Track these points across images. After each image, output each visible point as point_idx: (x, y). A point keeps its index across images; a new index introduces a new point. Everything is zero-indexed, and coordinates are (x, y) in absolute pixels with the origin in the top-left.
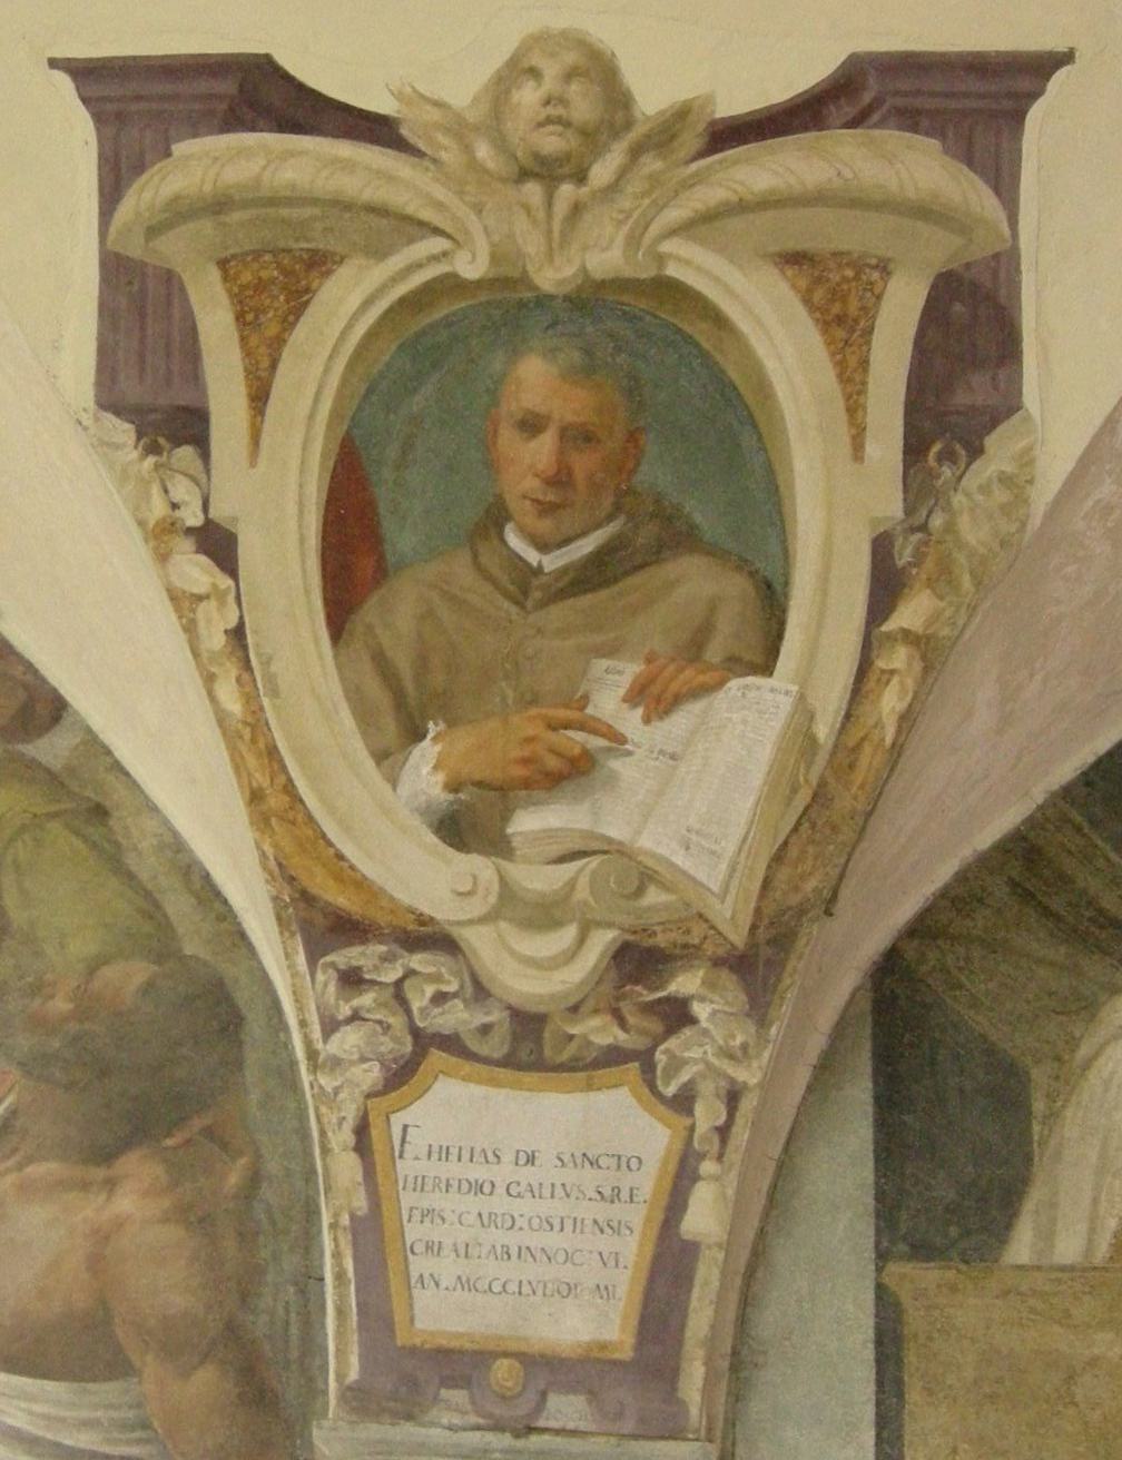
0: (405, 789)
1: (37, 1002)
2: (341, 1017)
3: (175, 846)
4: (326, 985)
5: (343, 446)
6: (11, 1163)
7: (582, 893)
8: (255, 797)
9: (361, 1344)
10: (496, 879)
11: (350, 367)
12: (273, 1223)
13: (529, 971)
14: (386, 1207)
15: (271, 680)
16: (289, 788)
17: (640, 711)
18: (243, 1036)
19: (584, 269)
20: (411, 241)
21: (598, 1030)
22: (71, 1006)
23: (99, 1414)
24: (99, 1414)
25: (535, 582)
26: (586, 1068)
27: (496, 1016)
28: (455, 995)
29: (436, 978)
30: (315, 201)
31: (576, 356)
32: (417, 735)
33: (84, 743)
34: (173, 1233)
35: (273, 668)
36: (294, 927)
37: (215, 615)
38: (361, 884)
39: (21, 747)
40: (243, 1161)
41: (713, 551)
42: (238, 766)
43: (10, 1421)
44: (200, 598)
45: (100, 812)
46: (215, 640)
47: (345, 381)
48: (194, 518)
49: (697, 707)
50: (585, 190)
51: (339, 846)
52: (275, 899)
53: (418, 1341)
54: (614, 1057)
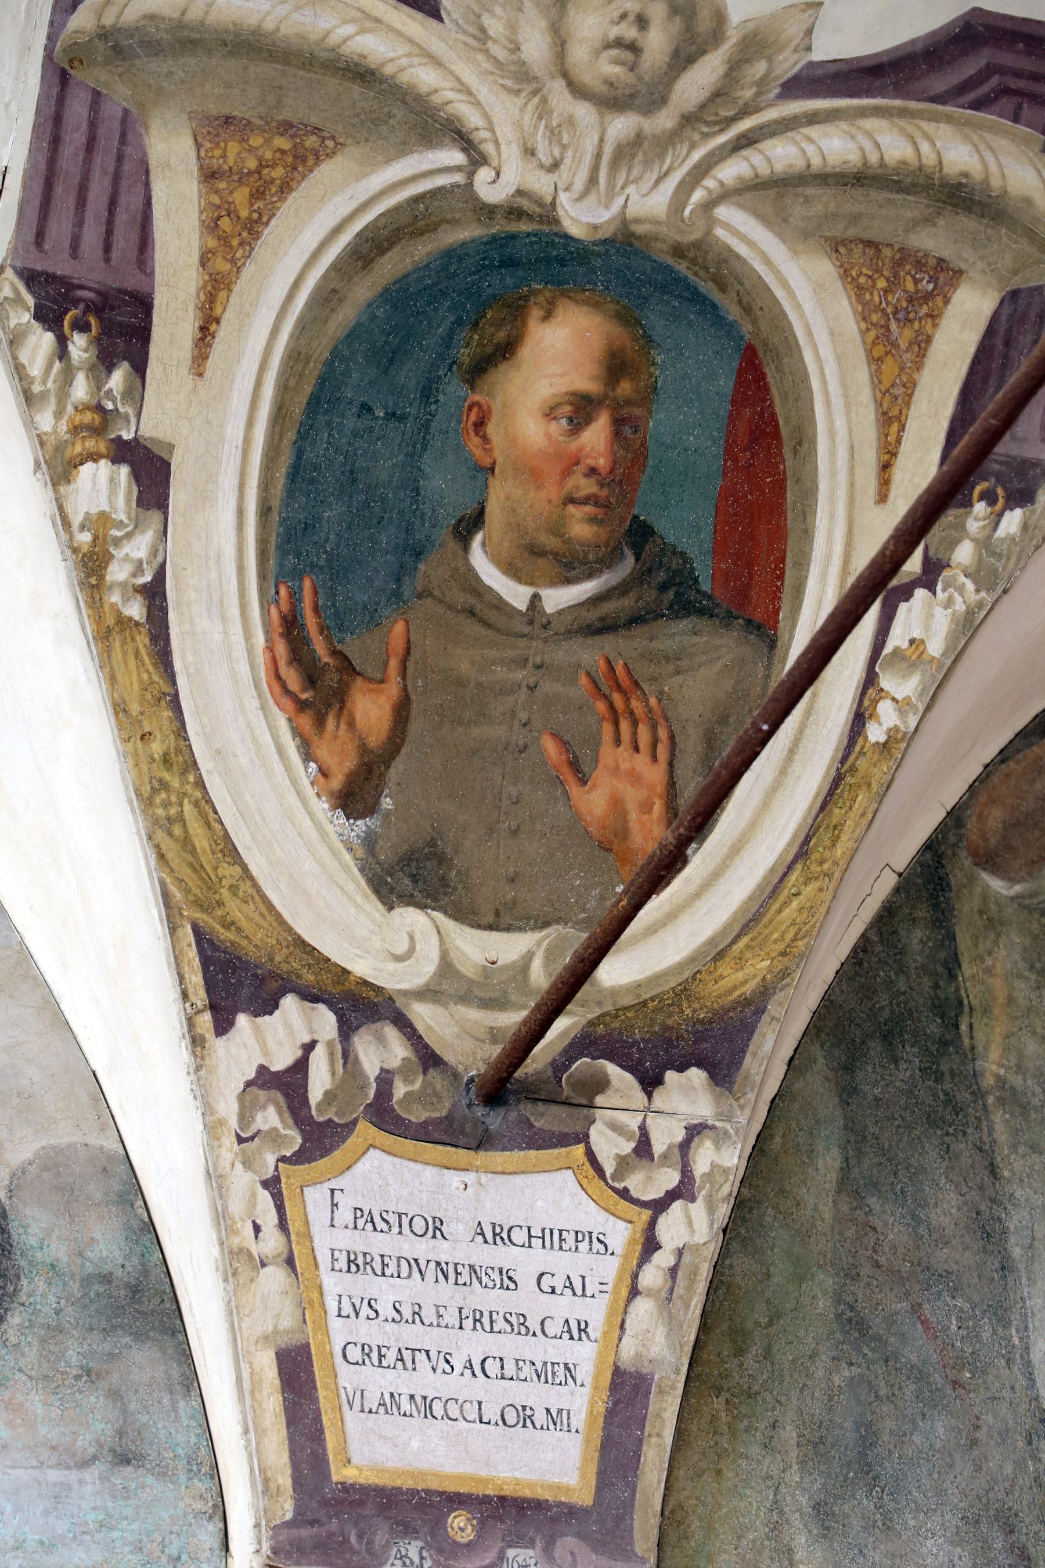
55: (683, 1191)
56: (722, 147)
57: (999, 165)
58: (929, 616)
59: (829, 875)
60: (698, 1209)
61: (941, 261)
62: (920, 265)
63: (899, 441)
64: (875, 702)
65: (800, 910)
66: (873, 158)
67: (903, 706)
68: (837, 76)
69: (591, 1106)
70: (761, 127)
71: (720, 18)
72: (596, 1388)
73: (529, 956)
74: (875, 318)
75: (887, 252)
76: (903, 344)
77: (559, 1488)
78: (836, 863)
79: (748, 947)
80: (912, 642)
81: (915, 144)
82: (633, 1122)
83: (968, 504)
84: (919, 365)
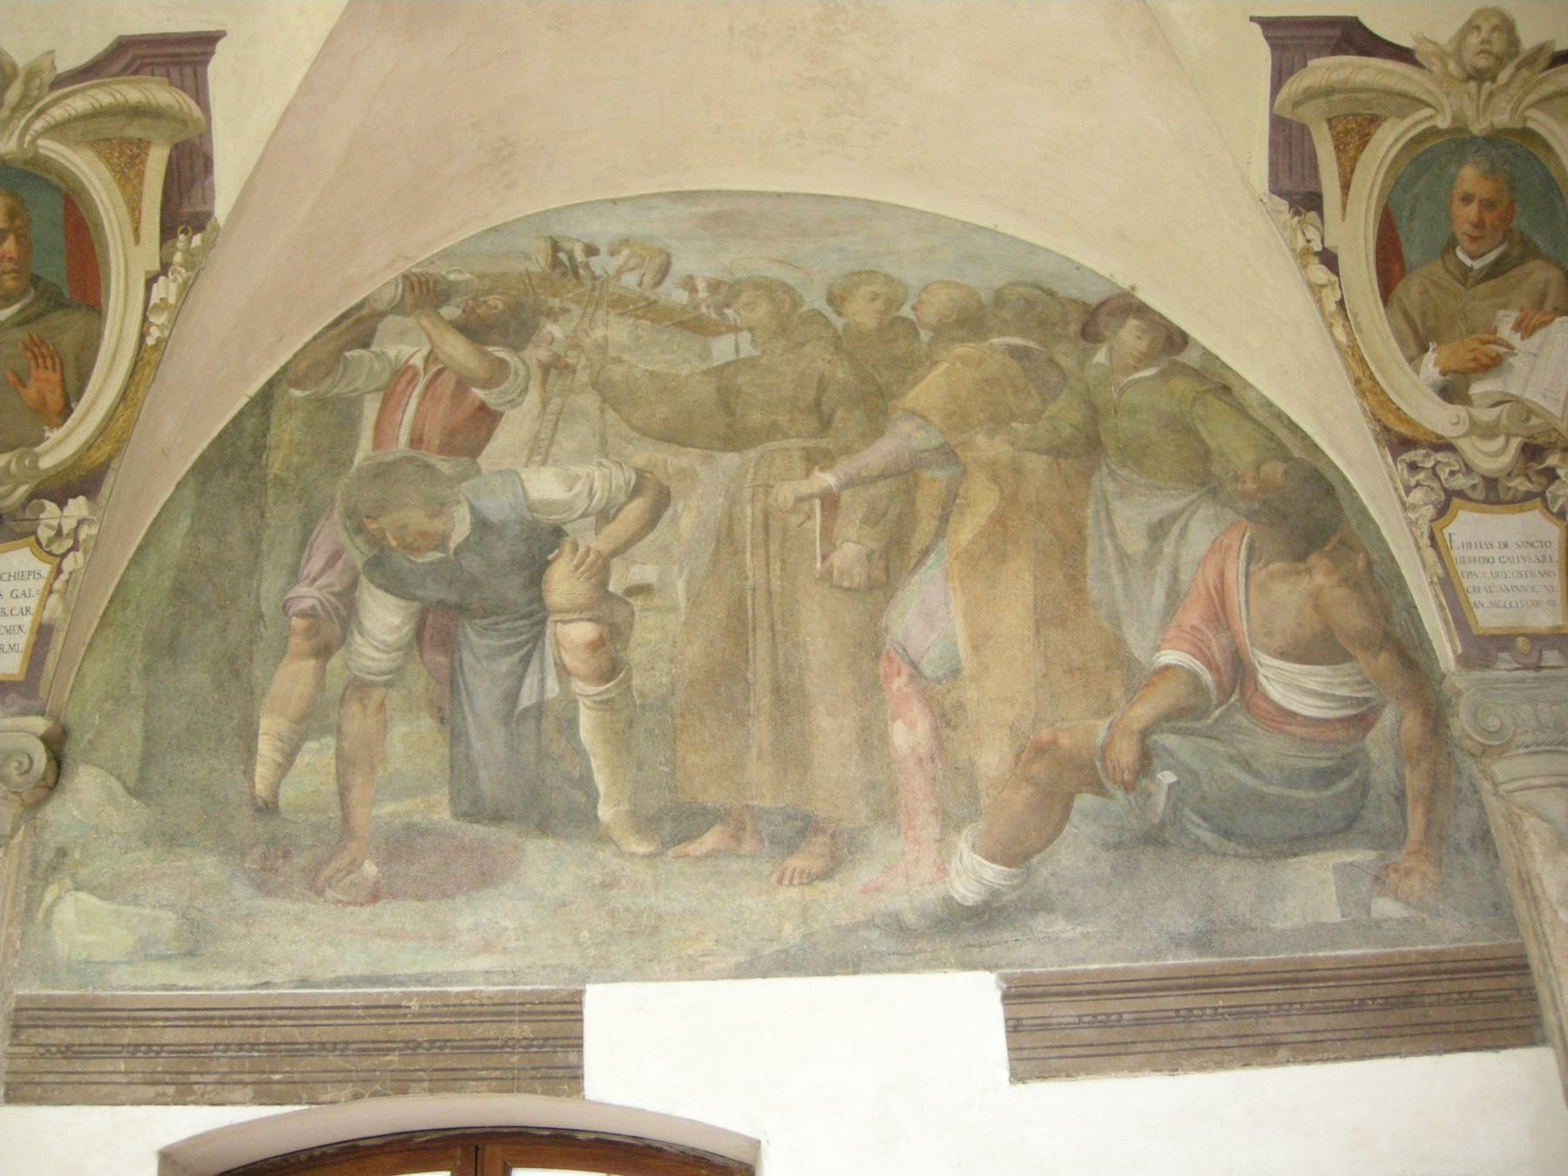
0: (1423, 375)
1: (1239, 486)
6: (1261, 564)
7: (1504, 421)
8: (1357, 382)
9: (1459, 635)
10: (1467, 416)
11: (1387, 172)
13: (1489, 459)
14: (1451, 571)
15: (1358, 324)
16: (1372, 377)
17: (1519, 335)
19: (1492, 123)
20: (1417, 110)
21: (1521, 484)
22: (1255, 486)
23: (1347, 679)
24: (1347, 679)
25: (1470, 274)
26: (1519, 502)
27: (1477, 480)
28: (1458, 471)
29: (1449, 464)
30: (1374, 90)
31: (1487, 166)
32: (1425, 349)
35: (1359, 319)
37: (1331, 295)
38: (1409, 422)
39: (1178, 358)
40: (1361, 555)
41: (1547, 259)
42: (1348, 368)
43: (1309, 686)
44: (1322, 286)
45: (1226, 389)
46: (1331, 306)
47: (1385, 178)
48: (1317, 247)
49: (1541, 333)
50: (1494, 86)
52: (1374, 430)
53: (1482, 632)
54: (1529, 496)
55: (74, 548)
56: (32, 116)
59: (136, 405)
60: (80, 554)
61: (140, 139)
62: (131, 143)
63: (140, 217)
64: (148, 328)
65: (124, 422)
66: (97, 105)
68: (69, 77)
69: (38, 519)
70: (45, 105)
71: (14, 67)
72: (31, 632)
73: (9, 463)
74: (117, 169)
75: (115, 141)
76: (132, 176)
77: (11, 675)
79: (102, 441)
82: (55, 523)
83: (176, 237)
84: (141, 183)
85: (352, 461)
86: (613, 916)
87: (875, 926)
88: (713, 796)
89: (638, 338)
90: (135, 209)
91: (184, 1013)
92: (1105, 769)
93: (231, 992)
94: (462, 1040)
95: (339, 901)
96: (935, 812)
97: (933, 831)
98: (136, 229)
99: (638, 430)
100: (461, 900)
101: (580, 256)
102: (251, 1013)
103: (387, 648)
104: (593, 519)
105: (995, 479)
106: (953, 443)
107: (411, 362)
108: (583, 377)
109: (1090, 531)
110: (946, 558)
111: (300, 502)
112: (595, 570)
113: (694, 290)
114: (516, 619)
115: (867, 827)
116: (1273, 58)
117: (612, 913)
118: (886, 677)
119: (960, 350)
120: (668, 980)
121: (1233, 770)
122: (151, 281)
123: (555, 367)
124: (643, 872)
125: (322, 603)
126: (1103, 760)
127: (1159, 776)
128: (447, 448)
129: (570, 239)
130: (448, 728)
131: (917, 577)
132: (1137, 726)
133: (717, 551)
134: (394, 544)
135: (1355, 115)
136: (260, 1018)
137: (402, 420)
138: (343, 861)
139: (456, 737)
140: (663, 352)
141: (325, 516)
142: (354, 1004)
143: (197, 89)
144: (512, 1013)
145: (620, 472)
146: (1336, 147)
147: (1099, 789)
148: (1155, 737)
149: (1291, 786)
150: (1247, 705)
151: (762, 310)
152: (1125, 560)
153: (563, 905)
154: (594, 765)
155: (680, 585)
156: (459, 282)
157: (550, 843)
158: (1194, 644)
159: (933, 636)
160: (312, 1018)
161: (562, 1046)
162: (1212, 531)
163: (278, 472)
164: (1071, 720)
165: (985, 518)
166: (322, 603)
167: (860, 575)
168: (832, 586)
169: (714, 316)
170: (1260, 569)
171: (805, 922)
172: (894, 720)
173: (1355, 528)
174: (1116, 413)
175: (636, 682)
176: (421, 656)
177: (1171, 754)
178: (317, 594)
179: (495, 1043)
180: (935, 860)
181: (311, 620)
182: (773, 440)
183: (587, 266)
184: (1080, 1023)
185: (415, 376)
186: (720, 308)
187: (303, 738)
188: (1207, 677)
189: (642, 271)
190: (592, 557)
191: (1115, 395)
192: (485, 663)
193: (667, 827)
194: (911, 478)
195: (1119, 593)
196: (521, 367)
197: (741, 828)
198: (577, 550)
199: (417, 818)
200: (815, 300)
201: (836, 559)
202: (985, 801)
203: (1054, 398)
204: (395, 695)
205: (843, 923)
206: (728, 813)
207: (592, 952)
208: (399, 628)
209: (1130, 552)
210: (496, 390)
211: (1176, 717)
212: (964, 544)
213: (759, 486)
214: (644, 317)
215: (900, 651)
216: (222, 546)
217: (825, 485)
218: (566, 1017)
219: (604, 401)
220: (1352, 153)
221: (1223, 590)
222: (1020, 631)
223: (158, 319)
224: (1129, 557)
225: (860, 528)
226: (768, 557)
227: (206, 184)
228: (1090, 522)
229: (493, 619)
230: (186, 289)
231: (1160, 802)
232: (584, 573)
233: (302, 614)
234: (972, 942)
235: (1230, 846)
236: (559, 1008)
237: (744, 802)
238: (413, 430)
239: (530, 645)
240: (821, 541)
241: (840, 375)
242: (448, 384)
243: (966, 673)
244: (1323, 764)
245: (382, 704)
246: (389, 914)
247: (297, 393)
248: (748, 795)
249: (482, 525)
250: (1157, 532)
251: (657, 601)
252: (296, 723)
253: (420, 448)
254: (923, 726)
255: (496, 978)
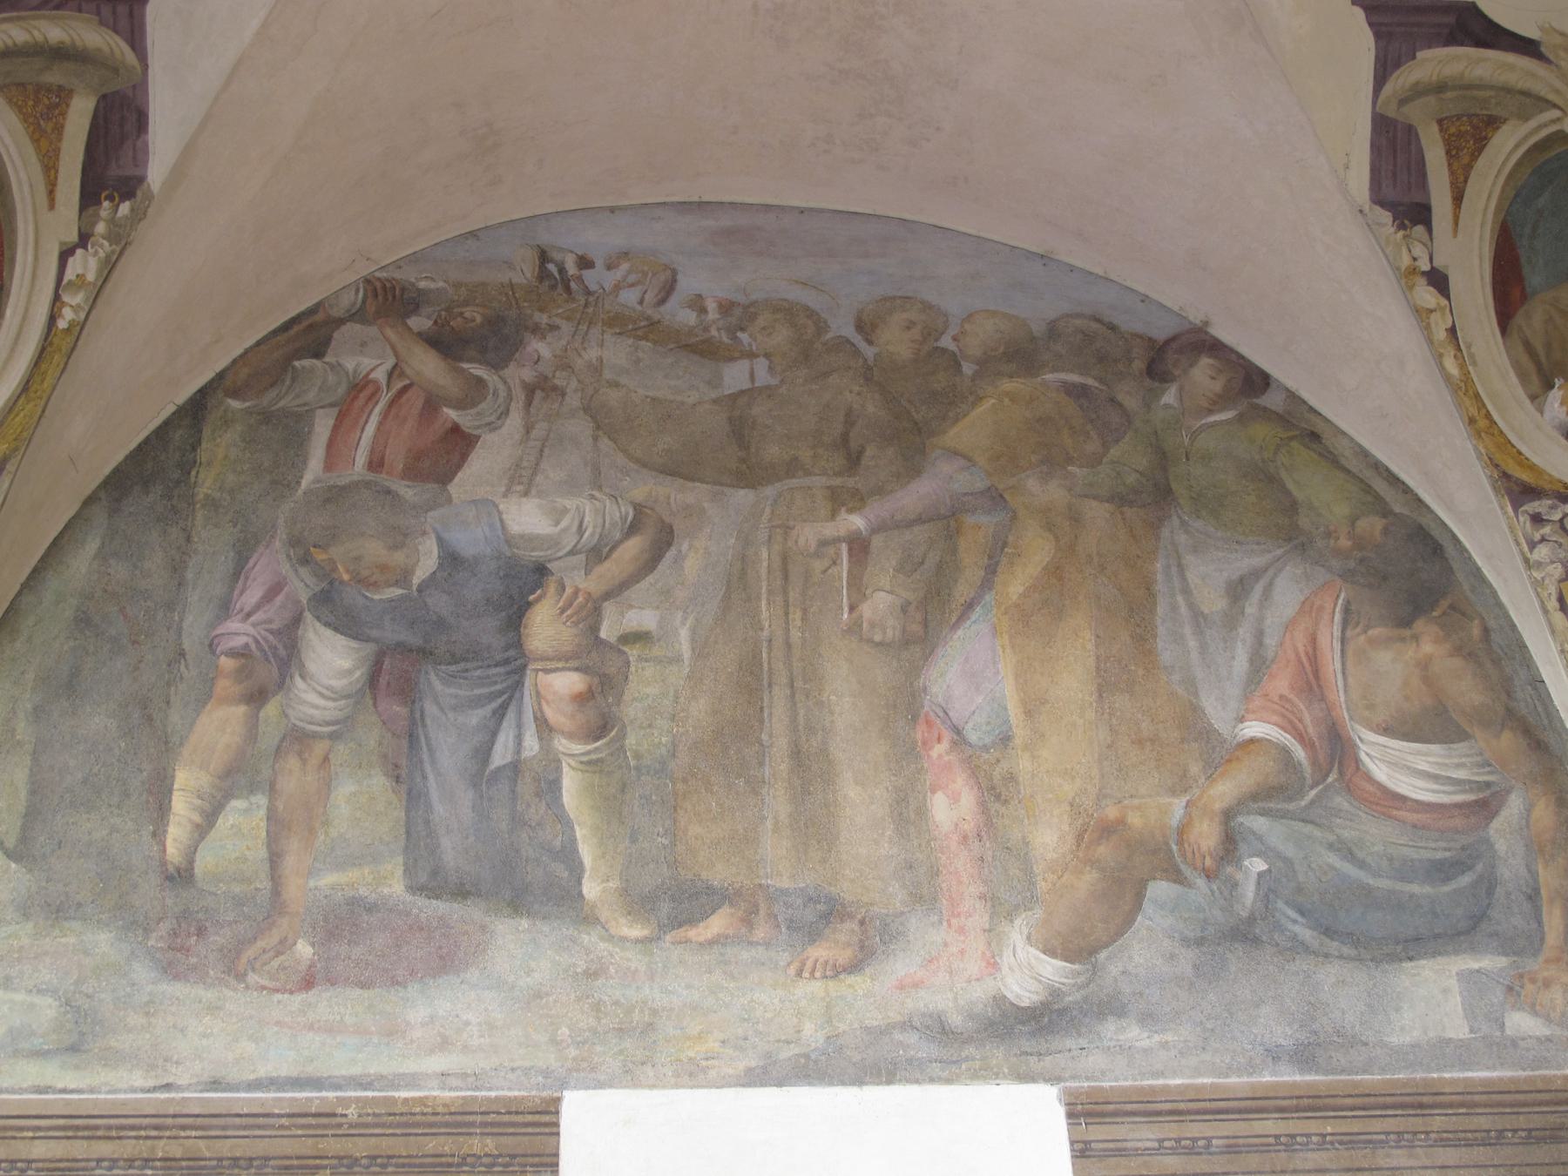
0: (1547, 415)
1: (1332, 542)
2: (1536, 540)
3: (1364, 454)
4: (1525, 523)
5: (1501, 227)
6: (1358, 630)
8: (1472, 421)
12: (1506, 654)
15: (1472, 356)
16: (1488, 416)
18: (1447, 555)
20: (1541, 112)
23: (1464, 760)
24: (1464, 760)
30: (1492, 87)
32: (1550, 386)
33: (1288, 397)
34: (1457, 662)
35: (1473, 350)
36: (1503, 492)
38: (1532, 468)
40: (1476, 622)
43: (1420, 767)
44: (1432, 311)
45: (1315, 436)
46: (1440, 335)
47: (1503, 190)
48: (1426, 267)
51: (1518, 446)
57: (79, 35)
58: (86, 261)
61: (60, 86)
62: (49, 90)
63: (56, 178)
64: (60, 309)
65: (25, 416)
66: (10, 43)
67: (76, 309)
74: (31, 120)
75: (30, 87)
76: (49, 130)
78: (44, 391)
80: (78, 276)
81: (30, 32)
83: (99, 203)
84: (60, 140)
85: (299, 483)
86: (598, 1010)
87: (914, 1028)
88: (720, 874)
89: (638, 361)
90: (50, 168)
91: (61, 1122)
92: (1184, 856)
93: (122, 1096)
94: (409, 1156)
95: (263, 988)
96: (982, 897)
97: (980, 919)
98: (51, 193)
99: (637, 461)
100: (413, 989)
101: (572, 270)
102: (146, 1121)
103: (336, 695)
104: (582, 557)
105: (1049, 527)
106: (1001, 487)
107: (372, 376)
108: (573, 400)
109: (1160, 586)
110: (994, 612)
111: (235, 526)
112: (584, 613)
113: (703, 310)
114: (489, 666)
115: (902, 913)
116: (1376, 48)
117: (597, 1007)
118: (924, 743)
119: (1007, 385)
120: (664, 1087)
121: (1333, 859)
122: (65, 255)
123: (540, 388)
124: (634, 959)
125: (257, 642)
126: (1180, 843)
127: (1246, 863)
128: (414, 472)
129: (561, 250)
130: (404, 788)
131: (960, 632)
132: (1218, 806)
133: (727, 598)
134: (346, 577)
135: (1470, 116)
136: (156, 1128)
137: (360, 438)
138: (269, 941)
139: (414, 798)
140: (666, 376)
141: (264, 543)
142: (277, 1111)
143: (132, 32)
144: (472, 1124)
145: (615, 507)
146: (1448, 152)
147: (1177, 877)
148: (1240, 819)
149: (1403, 879)
150: (1348, 786)
151: (782, 336)
152: (1201, 620)
153: (538, 995)
154: (578, 834)
155: (684, 633)
156: (430, 291)
157: (525, 923)
158: (1284, 716)
159: (980, 700)
160: (224, 1128)
161: (532, 1165)
162: (1301, 590)
163: (210, 491)
164: (1143, 797)
165: (1039, 569)
166: (257, 642)
167: (894, 628)
168: (861, 639)
169: (725, 339)
170: (1358, 635)
171: (829, 1021)
172: (933, 792)
173: (1469, 593)
174: (1188, 459)
175: (631, 741)
176: (375, 705)
177: (1260, 838)
178: (251, 630)
179: (450, 1160)
180: (983, 953)
181: (243, 661)
182: (794, 476)
183: (580, 279)
184: (1160, 1149)
185: (378, 389)
186: (732, 331)
187: (228, 795)
188: (1300, 753)
189: (645, 288)
190: (580, 599)
191: (1187, 441)
192: (451, 715)
193: (665, 908)
194: (952, 523)
195: (1194, 655)
196: (501, 386)
197: (754, 910)
198: (564, 590)
199: (363, 891)
200: (841, 326)
201: (866, 610)
202: (1042, 886)
203: (1117, 441)
204: (342, 751)
205: (875, 1023)
206: (738, 893)
207: (573, 1052)
208: (350, 672)
209: (1206, 611)
210: (473, 411)
211: (1263, 797)
212: (1015, 598)
213: (778, 526)
214: (645, 338)
215: (941, 714)
216: (137, 572)
217: (854, 527)
218: (537, 1130)
219: (598, 427)
220: (1466, 160)
221: (1316, 658)
222: (1080, 696)
223: (74, 299)
224: (1205, 617)
225: (894, 576)
226: (786, 602)
227: (139, 143)
228: (1160, 577)
229: (462, 665)
230: (109, 267)
231: (1249, 892)
232: (569, 617)
233: (232, 653)
234: (1029, 1051)
235: (1333, 946)
236: (530, 1118)
237: (757, 881)
238: (372, 451)
239: (505, 696)
240: (848, 589)
241: (871, 409)
242: (415, 401)
243: (1018, 741)
244: (1439, 855)
245: (326, 759)
246: (325, 1003)
247: (235, 404)
248: (762, 873)
249: (451, 560)
250: (1238, 590)
251: (656, 651)
252: (219, 778)
253: (381, 473)
254: (968, 800)
255: (454, 1082)
